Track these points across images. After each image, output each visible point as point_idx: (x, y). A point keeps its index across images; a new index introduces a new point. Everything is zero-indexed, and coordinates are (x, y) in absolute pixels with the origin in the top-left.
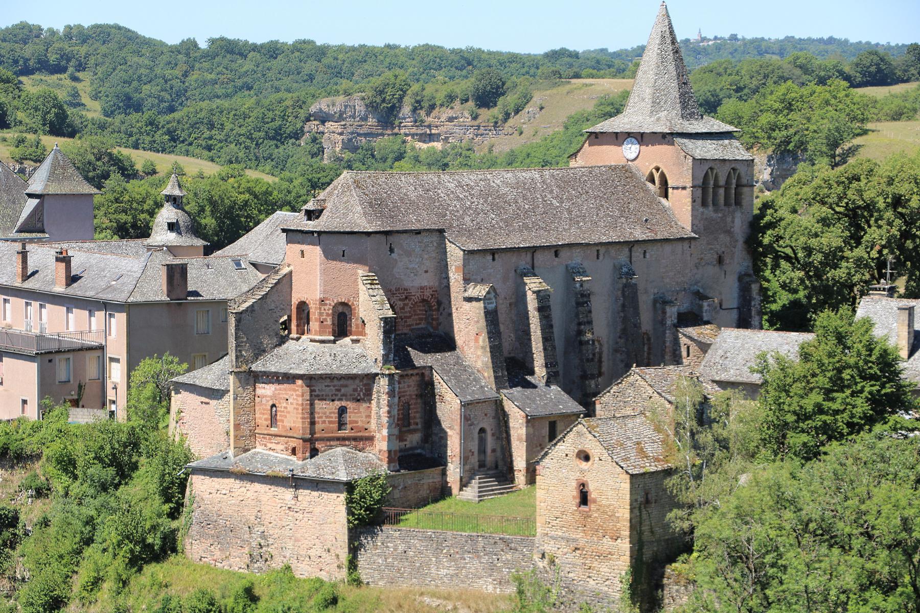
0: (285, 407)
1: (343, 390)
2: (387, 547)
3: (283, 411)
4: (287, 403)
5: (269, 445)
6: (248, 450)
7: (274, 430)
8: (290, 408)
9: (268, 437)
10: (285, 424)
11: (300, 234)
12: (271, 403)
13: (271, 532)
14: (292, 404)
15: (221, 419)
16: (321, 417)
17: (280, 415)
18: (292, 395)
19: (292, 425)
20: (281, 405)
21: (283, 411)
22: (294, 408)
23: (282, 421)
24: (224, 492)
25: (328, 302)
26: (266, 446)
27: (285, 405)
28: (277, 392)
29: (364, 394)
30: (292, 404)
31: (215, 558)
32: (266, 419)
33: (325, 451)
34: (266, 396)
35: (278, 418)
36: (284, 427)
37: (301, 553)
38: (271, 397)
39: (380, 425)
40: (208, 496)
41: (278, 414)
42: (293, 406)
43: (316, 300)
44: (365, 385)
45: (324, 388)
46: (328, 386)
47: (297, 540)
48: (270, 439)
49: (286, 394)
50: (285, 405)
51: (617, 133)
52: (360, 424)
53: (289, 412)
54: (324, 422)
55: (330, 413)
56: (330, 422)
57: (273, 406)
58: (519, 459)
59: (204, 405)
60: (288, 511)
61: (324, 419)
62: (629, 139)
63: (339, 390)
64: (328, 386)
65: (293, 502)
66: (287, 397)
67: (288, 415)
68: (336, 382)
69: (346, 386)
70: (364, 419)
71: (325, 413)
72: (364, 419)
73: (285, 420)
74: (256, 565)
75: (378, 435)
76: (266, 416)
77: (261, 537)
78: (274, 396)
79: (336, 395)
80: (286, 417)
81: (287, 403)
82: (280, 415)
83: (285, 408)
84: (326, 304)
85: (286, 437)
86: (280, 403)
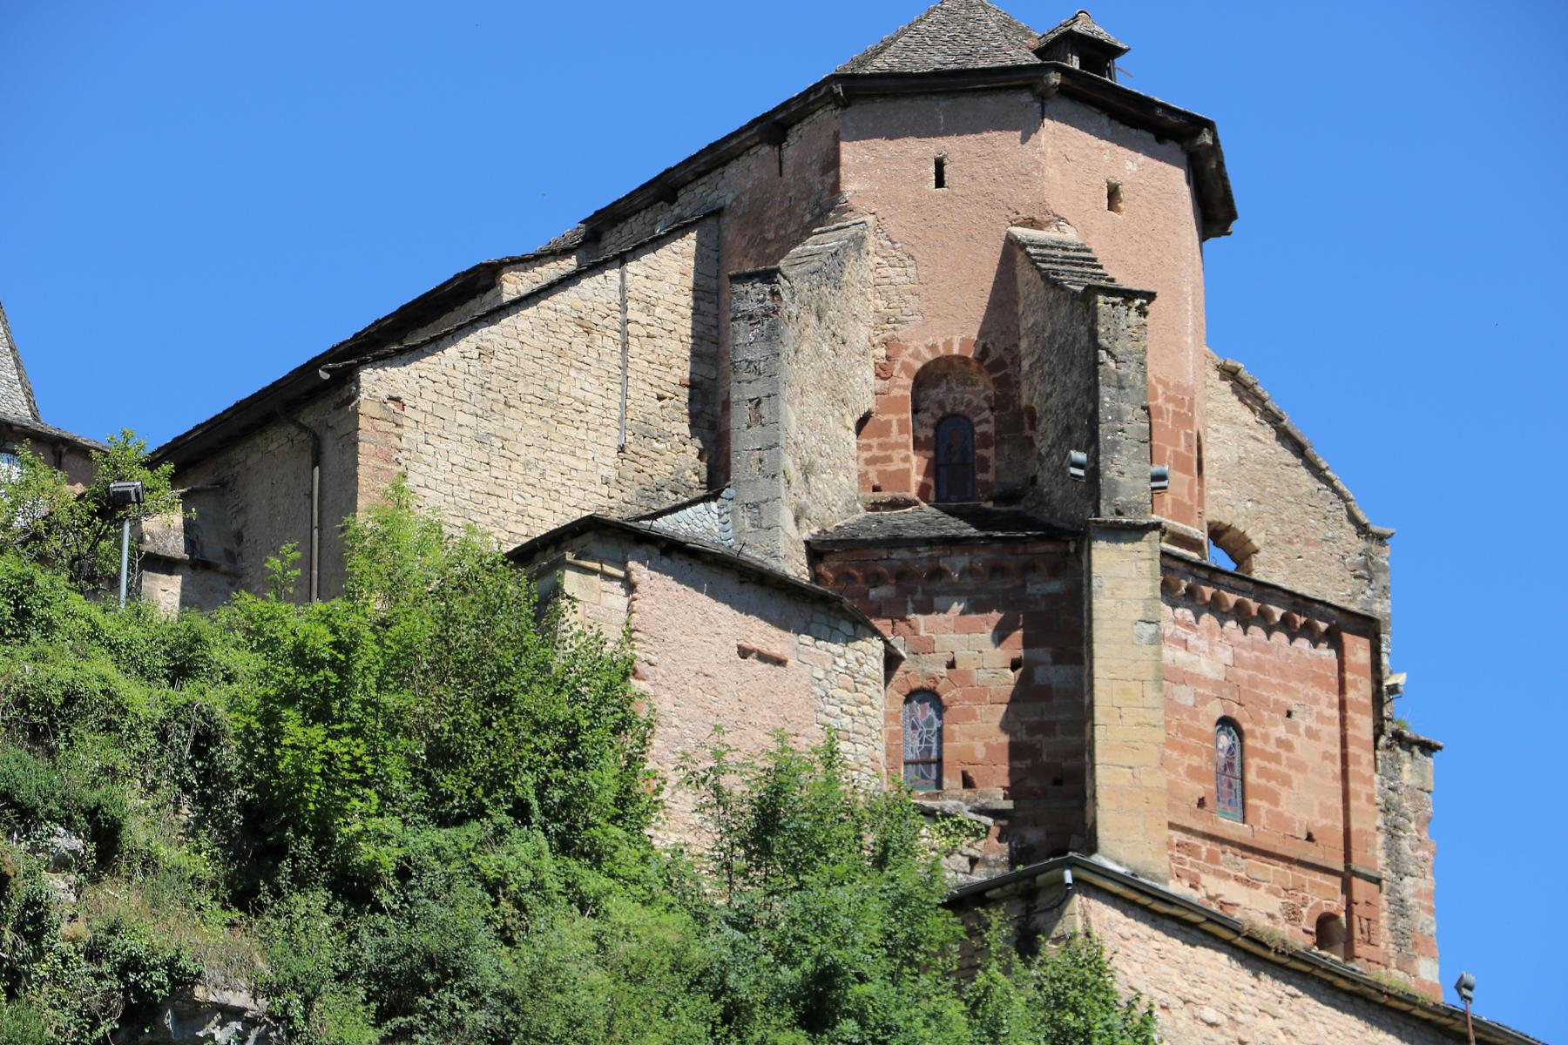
0: (1280, 743)
3: (1275, 758)
4: (1293, 729)
7: (1229, 826)
9: (1205, 847)
10: (1285, 808)
18: (1315, 700)
20: (1265, 732)
21: (1275, 758)
23: (1273, 798)
24: (1210, 1014)
27: (1280, 731)
32: (1193, 773)
36: (1278, 819)
38: (1217, 685)
41: (1253, 763)
48: (1212, 858)
49: (1287, 690)
50: (1280, 731)
53: (1300, 766)
73: (1284, 793)
76: (1195, 761)
80: (1286, 782)
81: (1293, 729)
82: (1262, 772)
85: (1289, 860)
86: (1258, 722)
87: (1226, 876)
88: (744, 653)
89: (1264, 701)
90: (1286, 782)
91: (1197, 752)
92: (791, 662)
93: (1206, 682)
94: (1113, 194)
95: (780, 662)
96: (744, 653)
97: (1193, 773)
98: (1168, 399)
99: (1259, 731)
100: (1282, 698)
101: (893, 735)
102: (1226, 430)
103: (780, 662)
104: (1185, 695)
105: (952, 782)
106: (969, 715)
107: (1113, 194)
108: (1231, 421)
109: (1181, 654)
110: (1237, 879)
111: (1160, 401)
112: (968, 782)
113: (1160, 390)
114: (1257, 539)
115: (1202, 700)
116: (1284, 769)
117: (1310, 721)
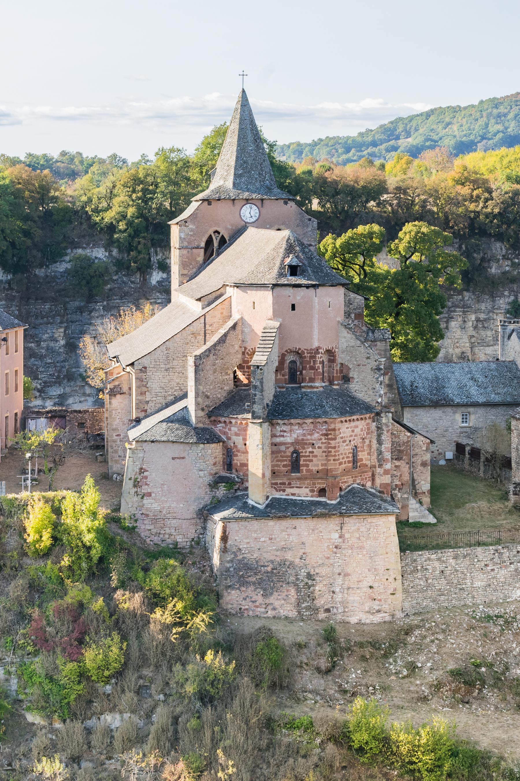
0: (310, 452)
1: (356, 430)
2: (426, 569)
5: (289, 491)
6: (268, 497)
8: (316, 451)
10: (310, 468)
11: (291, 288)
12: (292, 449)
13: (317, 571)
14: (319, 447)
15: (200, 472)
16: (343, 458)
17: (304, 461)
19: (320, 468)
21: (309, 456)
22: (323, 452)
23: (307, 466)
24: (263, 539)
25: (320, 351)
26: (284, 491)
27: (311, 449)
28: (300, 438)
29: (368, 434)
30: (319, 447)
31: (257, 604)
32: (284, 466)
33: (345, 489)
34: (284, 444)
35: (301, 463)
36: (307, 471)
37: (352, 586)
38: (292, 444)
39: (381, 461)
40: (245, 546)
41: (302, 459)
42: (321, 450)
43: (311, 349)
44: (368, 424)
45: (346, 430)
46: (347, 428)
47: (347, 575)
51: (234, 200)
52: (364, 462)
53: (316, 456)
54: (345, 462)
55: (349, 453)
56: (349, 462)
57: (295, 452)
58: (423, 482)
59: (178, 460)
60: (335, 550)
61: (345, 459)
62: (248, 206)
63: (353, 431)
64: (347, 428)
65: (341, 540)
66: (314, 442)
67: (314, 459)
68: (353, 424)
69: (357, 427)
70: (366, 456)
71: (345, 454)
72: (366, 456)
74: (303, 605)
75: (378, 470)
76: (285, 463)
77: (307, 578)
78: (297, 442)
79: (351, 436)
82: (304, 461)
83: (313, 452)
84: (319, 353)
87: (293, 487)
88: (173, 459)
89: (306, 444)
90: (311, 461)
91: (286, 460)
92: (187, 457)
93: (289, 443)
94: (293, 307)
95: (183, 458)
96: (173, 459)
97: (284, 466)
98: (308, 353)
99: (304, 451)
100: (311, 441)
101: (224, 459)
102: (343, 340)
103: (183, 458)
104: (283, 448)
105: (234, 471)
106: (237, 455)
107: (293, 307)
108: (345, 337)
109: (282, 439)
110: (297, 487)
111: (306, 354)
112: (237, 471)
113: (306, 351)
114: (351, 366)
115: (288, 448)
116: (311, 458)
117: (320, 445)
